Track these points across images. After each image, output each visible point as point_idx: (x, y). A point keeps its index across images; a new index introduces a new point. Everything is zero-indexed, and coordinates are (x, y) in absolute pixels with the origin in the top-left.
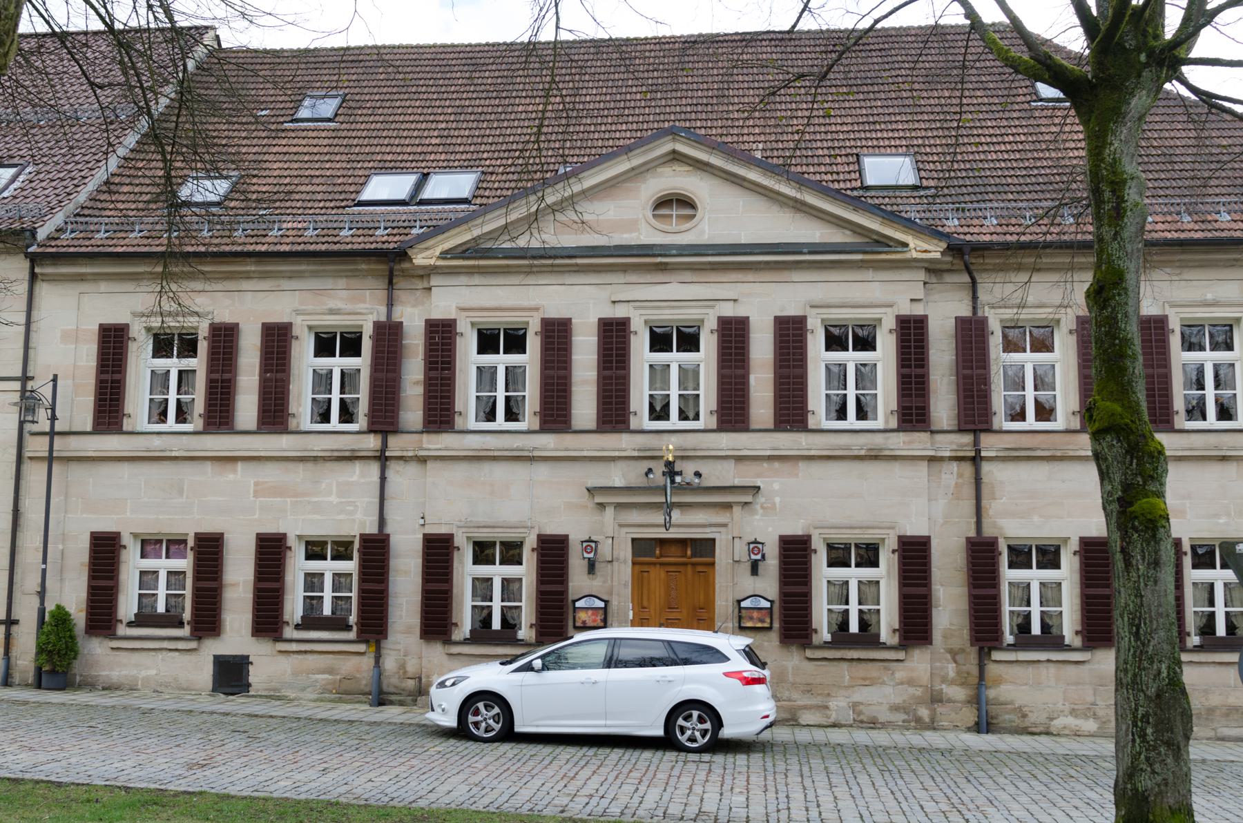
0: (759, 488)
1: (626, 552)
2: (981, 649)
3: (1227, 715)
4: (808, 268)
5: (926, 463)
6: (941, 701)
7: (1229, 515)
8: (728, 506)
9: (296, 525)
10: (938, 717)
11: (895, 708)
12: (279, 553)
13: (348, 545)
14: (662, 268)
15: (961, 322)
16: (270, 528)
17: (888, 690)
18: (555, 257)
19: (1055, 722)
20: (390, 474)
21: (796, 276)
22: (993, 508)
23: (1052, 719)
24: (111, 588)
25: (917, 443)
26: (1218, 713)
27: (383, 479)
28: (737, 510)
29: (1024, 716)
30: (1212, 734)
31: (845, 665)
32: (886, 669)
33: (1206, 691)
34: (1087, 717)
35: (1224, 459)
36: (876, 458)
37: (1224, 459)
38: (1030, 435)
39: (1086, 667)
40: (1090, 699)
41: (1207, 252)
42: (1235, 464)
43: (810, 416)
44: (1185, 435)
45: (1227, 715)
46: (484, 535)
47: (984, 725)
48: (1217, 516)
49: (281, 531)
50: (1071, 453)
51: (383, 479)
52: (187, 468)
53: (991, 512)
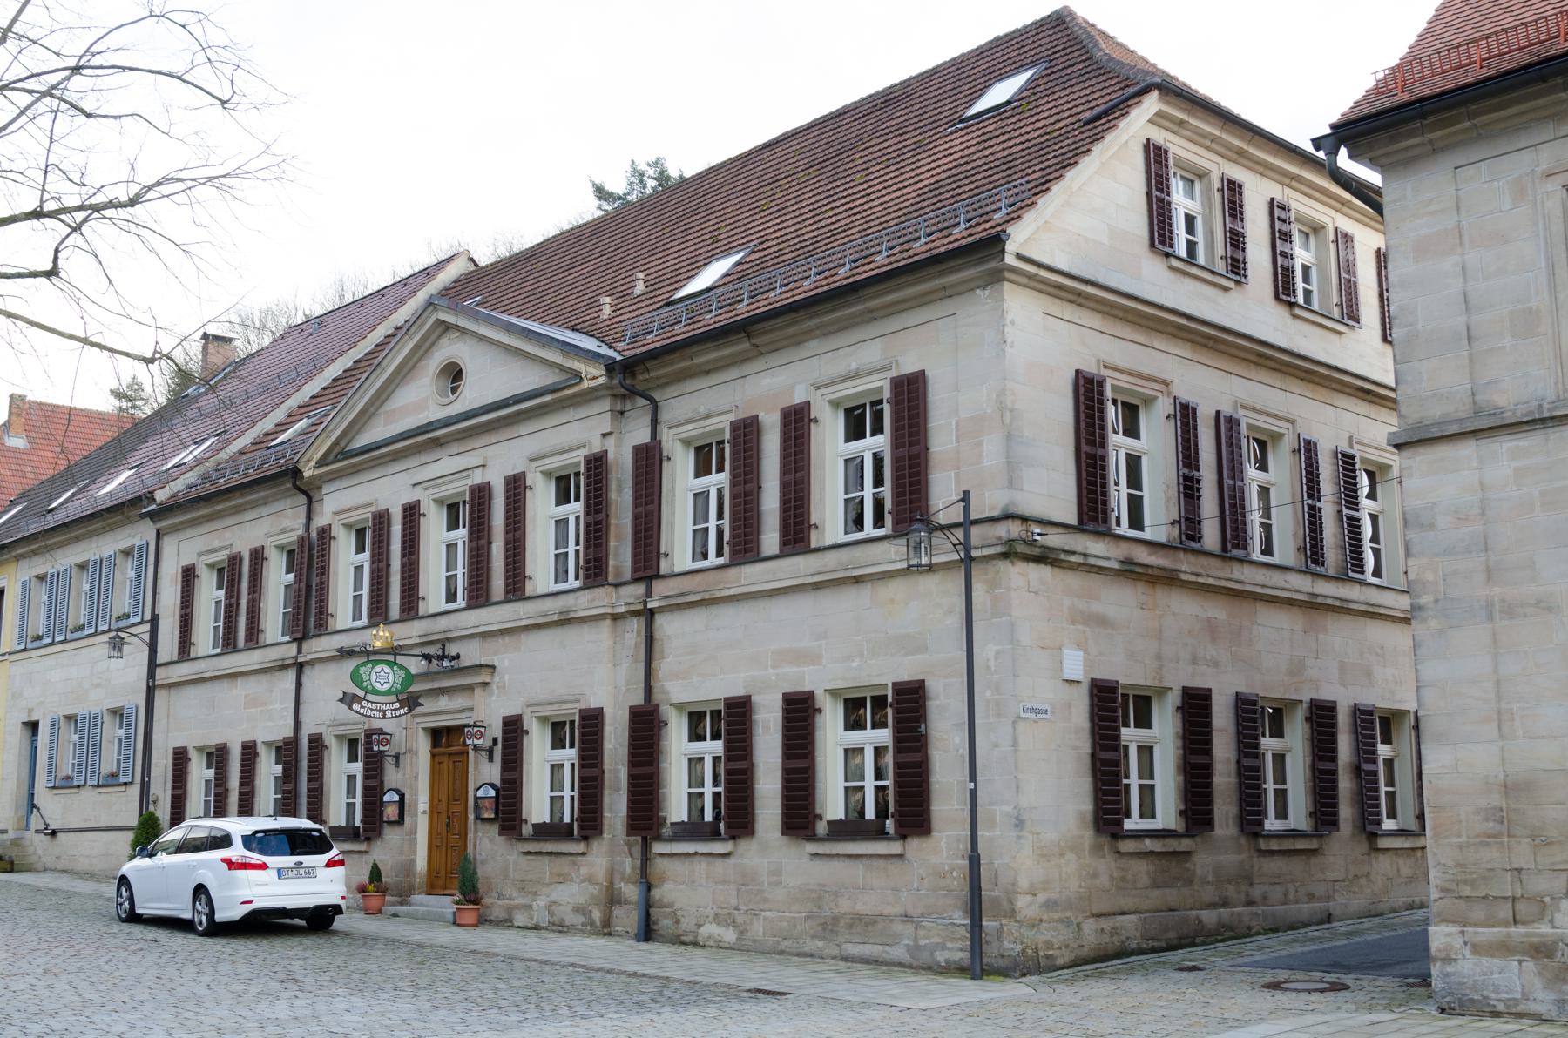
0: (493, 667)
1: (424, 745)
2: (644, 839)
3: (851, 926)
4: (529, 418)
5: (608, 622)
6: (619, 902)
7: (862, 656)
8: (469, 688)
9: (823, 678)
10: (614, 921)
11: (577, 910)
12: (805, 719)
13: (879, 702)
14: (437, 443)
15: (638, 450)
16: (248, 738)
17: (574, 888)
18: (379, 447)
19: (702, 930)
20: (305, 680)
21: (523, 429)
22: (665, 666)
23: (699, 926)
24: (651, 776)
25: (598, 600)
26: (842, 923)
27: (299, 685)
28: (478, 691)
29: (678, 921)
30: (835, 951)
31: (546, 859)
32: (574, 863)
33: (836, 894)
34: (727, 925)
35: (857, 580)
36: (569, 622)
37: (857, 580)
38: (689, 577)
39: (732, 861)
40: (734, 902)
41: (833, 310)
42: (869, 586)
43: (527, 582)
44: (820, 554)
45: (851, 926)
46: (557, 712)
47: (647, 933)
48: (850, 658)
49: (807, 689)
50: (718, 594)
51: (299, 685)
52: (217, 686)
53: (661, 674)
